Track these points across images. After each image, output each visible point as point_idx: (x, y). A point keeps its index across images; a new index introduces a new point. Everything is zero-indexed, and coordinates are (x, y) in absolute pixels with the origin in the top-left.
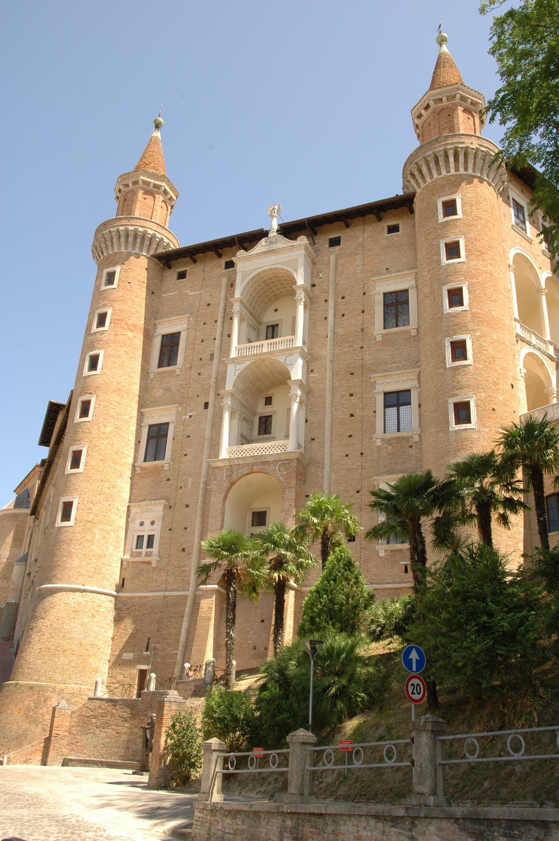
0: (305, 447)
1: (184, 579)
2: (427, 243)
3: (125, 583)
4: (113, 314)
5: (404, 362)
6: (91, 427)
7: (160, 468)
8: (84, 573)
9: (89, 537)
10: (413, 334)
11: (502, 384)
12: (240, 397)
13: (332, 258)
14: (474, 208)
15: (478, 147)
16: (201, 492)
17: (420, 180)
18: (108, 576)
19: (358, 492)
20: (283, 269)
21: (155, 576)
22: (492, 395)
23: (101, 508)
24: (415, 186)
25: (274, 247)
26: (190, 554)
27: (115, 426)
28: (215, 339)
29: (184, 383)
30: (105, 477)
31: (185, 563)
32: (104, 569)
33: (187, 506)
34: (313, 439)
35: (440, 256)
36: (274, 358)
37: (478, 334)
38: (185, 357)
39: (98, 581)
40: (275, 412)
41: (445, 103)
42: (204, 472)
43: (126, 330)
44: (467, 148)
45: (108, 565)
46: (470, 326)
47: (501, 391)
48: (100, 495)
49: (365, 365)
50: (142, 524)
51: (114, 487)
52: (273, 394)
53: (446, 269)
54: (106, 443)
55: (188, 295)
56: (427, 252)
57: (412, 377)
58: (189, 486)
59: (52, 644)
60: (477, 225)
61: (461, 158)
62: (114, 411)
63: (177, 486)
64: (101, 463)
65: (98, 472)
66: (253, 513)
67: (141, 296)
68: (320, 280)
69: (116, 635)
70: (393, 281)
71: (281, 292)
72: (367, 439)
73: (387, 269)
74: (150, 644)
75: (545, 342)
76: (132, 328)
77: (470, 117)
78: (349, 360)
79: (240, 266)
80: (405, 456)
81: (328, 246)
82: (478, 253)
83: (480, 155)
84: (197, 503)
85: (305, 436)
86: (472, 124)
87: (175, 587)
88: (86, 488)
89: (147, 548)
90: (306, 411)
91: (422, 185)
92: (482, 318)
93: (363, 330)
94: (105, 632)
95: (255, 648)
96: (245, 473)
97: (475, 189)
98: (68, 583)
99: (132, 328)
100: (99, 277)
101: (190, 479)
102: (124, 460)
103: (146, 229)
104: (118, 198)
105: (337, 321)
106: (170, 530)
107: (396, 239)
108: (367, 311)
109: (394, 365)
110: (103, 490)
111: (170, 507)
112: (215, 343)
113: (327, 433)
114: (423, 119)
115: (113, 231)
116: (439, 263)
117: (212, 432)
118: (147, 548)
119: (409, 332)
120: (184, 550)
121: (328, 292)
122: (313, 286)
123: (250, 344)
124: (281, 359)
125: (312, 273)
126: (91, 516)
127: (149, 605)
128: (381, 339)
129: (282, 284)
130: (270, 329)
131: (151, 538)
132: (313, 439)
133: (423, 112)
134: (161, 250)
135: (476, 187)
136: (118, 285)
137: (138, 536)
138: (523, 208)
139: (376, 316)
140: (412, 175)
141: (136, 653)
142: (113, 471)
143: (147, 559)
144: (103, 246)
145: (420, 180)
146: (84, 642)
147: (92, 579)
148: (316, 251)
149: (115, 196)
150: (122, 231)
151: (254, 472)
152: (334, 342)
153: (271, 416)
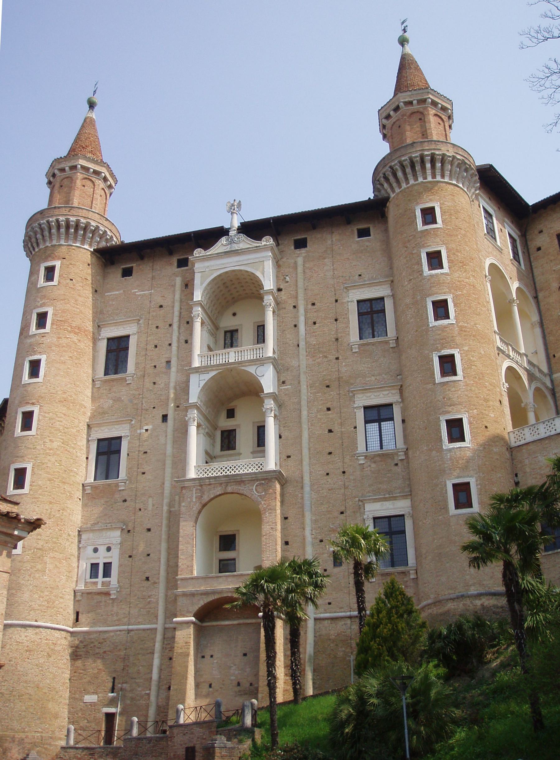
0: (280, 464)
1: (149, 611)
2: (406, 251)
3: (79, 617)
4: (54, 315)
5: (383, 375)
6: (36, 442)
7: (114, 488)
8: (36, 607)
9: (39, 567)
10: (391, 346)
11: (492, 401)
12: (203, 409)
13: (300, 261)
14: (453, 217)
15: (454, 154)
16: (165, 515)
17: (395, 185)
18: (61, 610)
19: (342, 513)
20: (247, 272)
21: (115, 609)
22: (484, 412)
23: (51, 533)
24: (389, 190)
25: (236, 247)
26: (155, 583)
27: (62, 441)
28: (170, 345)
29: (137, 393)
30: (54, 498)
31: (150, 593)
32: (57, 602)
33: (149, 530)
34: (289, 457)
35: (422, 265)
36: (243, 368)
37: (466, 348)
38: (137, 364)
39: (51, 616)
40: (239, 426)
41: (416, 107)
42: (167, 491)
43: (70, 332)
44: (444, 155)
45: (61, 598)
46: (458, 340)
47: (492, 407)
48: (50, 519)
49: (342, 378)
50: (96, 550)
51: (63, 510)
52: (236, 406)
53: (429, 279)
54: (53, 459)
55: (135, 295)
56: (407, 261)
57: (394, 392)
58: (150, 507)
59: (5, 688)
60: (457, 235)
61: (438, 165)
62: (61, 424)
63: (135, 508)
64: (48, 482)
65: (46, 493)
66: (220, 536)
67: (84, 295)
68: (287, 284)
69: (74, 676)
70: (367, 289)
71: (240, 295)
72: (348, 457)
73: (360, 275)
74: (115, 684)
75: (520, 354)
76: (76, 330)
77: (441, 122)
78: (323, 372)
79: (198, 267)
80: (389, 475)
81: (293, 247)
82: (461, 265)
83: (456, 163)
84: (161, 526)
85: (280, 453)
86: (443, 129)
87: (140, 620)
88: (33, 512)
89: (104, 577)
90: (280, 426)
91: (397, 190)
92: (469, 332)
93: (337, 339)
94: (63, 673)
95: (239, 684)
96: (218, 493)
97: (452, 197)
98: (18, 620)
99: (76, 330)
100: (33, 272)
101: (150, 500)
102: (73, 478)
103: (88, 220)
104: (50, 183)
105: (308, 329)
106: (130, 557)
107: (367, 244)
108: (340, 320)
109: (373, 378)
110: (53, 513)
111: (129, 531)
112: (171, 349)
113: (305, 452)
115: (52, 222)
116: (421, 273)
117: (173, 448)
118: (104, 577)
119: (387, 342)
120: (147, 579)
121: (297, 298)
122: (279, 290)
123: (211, 353)
124: (251, 369)
125: (277, 277)
126: (41, 543)
127: (110, 641)
128: (357, 350)
129: (242, 286)
130: (229, 335)
131: (107, 566)
132: (289, 457)
133: (392, 113)
134: (103, 244)
135: (454, 196)
136: (59, 282)
137: (92, 564)
138: (490, 216)
139: (351, 325)
140: (386, 179)
141: (100, 695)
142: (62, 491)
143: (105, 589)
144: (39, 236)
145: (395, 185)
146: (41, 685)
147: (45, 614)
148: (281, 252)
149: (46, 181)
150: (62, 221)
151: (227, 493)
152: (306, 352)
153: (235, 430)
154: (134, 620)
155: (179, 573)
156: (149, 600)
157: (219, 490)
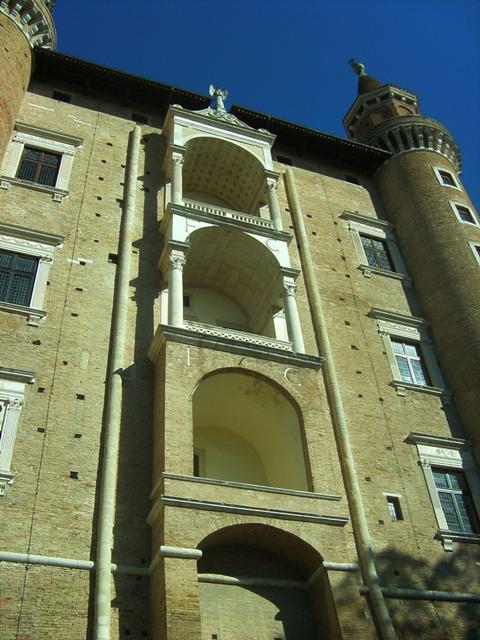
19: (389, 448)
33: (81, 397)
87: (54, 548)
93: (344, 258)
106: (41, 430)
111: (41, 390)
114: (374, 106)
124: (262, 239)
133: (378, 100)
154: (40, 545)
155: (166, 468)
156: (75, 513)
157: (229, 360)
